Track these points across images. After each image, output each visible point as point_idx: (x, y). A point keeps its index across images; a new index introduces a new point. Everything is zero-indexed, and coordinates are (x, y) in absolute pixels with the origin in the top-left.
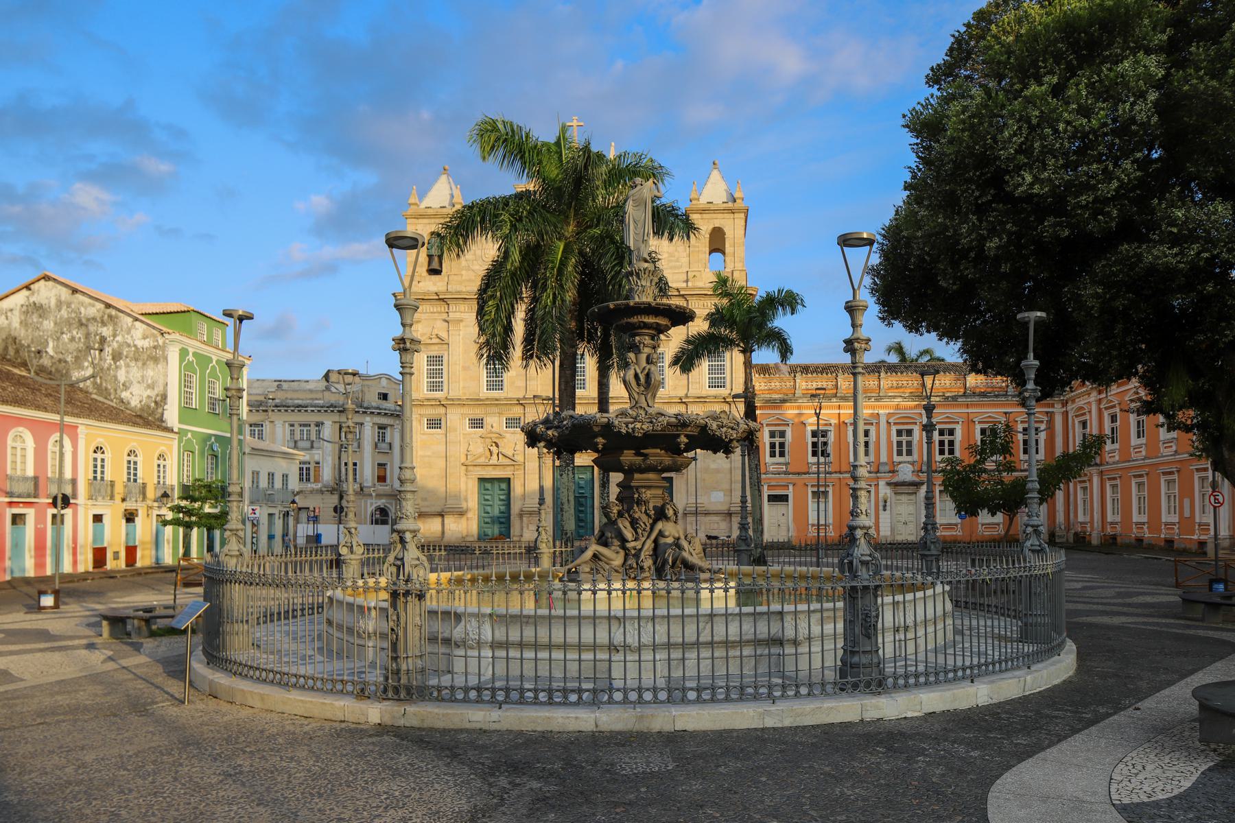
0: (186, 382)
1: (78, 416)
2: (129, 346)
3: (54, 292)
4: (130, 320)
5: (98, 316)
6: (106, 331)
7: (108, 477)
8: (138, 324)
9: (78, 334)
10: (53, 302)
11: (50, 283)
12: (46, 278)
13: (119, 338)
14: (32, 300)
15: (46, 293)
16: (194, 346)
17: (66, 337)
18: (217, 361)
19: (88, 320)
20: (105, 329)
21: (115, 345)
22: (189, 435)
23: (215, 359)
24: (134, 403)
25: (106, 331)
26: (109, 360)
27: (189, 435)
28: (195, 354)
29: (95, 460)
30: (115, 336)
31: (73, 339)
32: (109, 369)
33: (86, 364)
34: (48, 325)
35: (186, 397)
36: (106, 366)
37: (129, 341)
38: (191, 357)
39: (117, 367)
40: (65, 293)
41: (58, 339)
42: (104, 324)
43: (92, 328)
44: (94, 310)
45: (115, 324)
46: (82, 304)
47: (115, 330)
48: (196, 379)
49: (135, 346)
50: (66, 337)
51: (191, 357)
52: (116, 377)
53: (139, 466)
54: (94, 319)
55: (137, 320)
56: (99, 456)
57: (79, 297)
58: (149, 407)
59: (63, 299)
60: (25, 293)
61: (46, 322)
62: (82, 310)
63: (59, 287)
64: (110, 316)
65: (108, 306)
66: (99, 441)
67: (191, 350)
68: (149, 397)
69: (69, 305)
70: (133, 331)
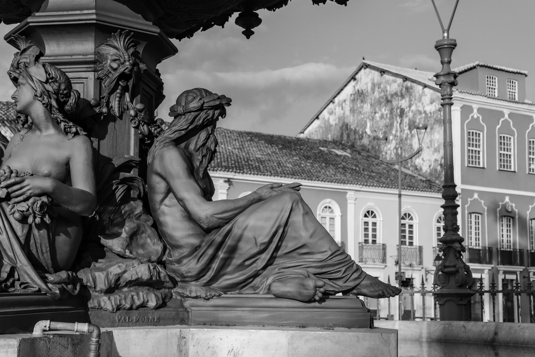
0: (471, 138)
1: (343, 182)
2: (420, 113)
3: (370, 77)
4: (420, 87)
5: (399, 89)
6: (404, 103)
7: (380, 240)
8: (426, 90)
9: (385, 111)
10: (370, 85)
11: (368, 70)
12: (367, 66)
13: (413, 108)
14: (357, 88)
15: (366, 78)
16: (477, 102)
17: (378, 116)
18: (510, 115)
19: (392, 96)
20: (404, 101)
21: (411, 115)
22: (476, 196)
23: (506, 112)
24: (425, 169)
25: (404, 103)
26: (407, 131)
27: (476, 196)
28: (480, 110)
29: (366, 223)
30: (410, 106)
31: (382, 117)
32: (406, 139)
33: (391, 137)
34: (367, 108)
35: (472, 156)
36: (404, 136)
37: (421, 109)
38: (475, 114)
39: (412, 136)
40: (377, 74)
41: (373, 118)
42: (403, 97)
43: (395, 103)
44: (394, 85)
45: (410, 95)
46: (387, 82)
47: (410, 100)
48: (483, 137)
49: (425, 112)
50: (378, 116)
51: (475, 114)
52: (411, 145)
53: (415, 229)
54: (396, 94)
55: (425, 86)
56: (370, 220)
57: (387, 77)
58: (436, 170)
59: (376, 81)
60: (352, 83)
61: (365, 106)
62: (388, 87)
63: (373, 72)
64: (407, 88)
65: (406, 79)
66: (370, 205)
67: (475, 107)
68: (436, 160)
69: (379, 85)
70: (423, 98)
